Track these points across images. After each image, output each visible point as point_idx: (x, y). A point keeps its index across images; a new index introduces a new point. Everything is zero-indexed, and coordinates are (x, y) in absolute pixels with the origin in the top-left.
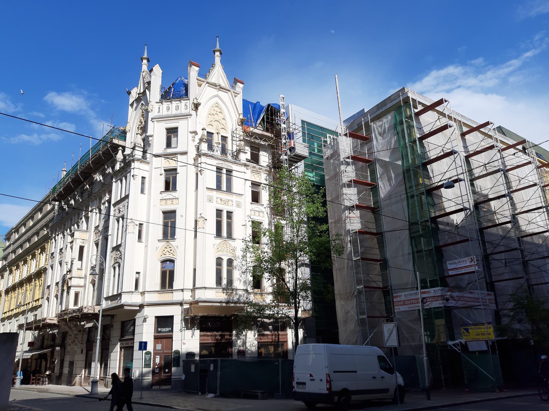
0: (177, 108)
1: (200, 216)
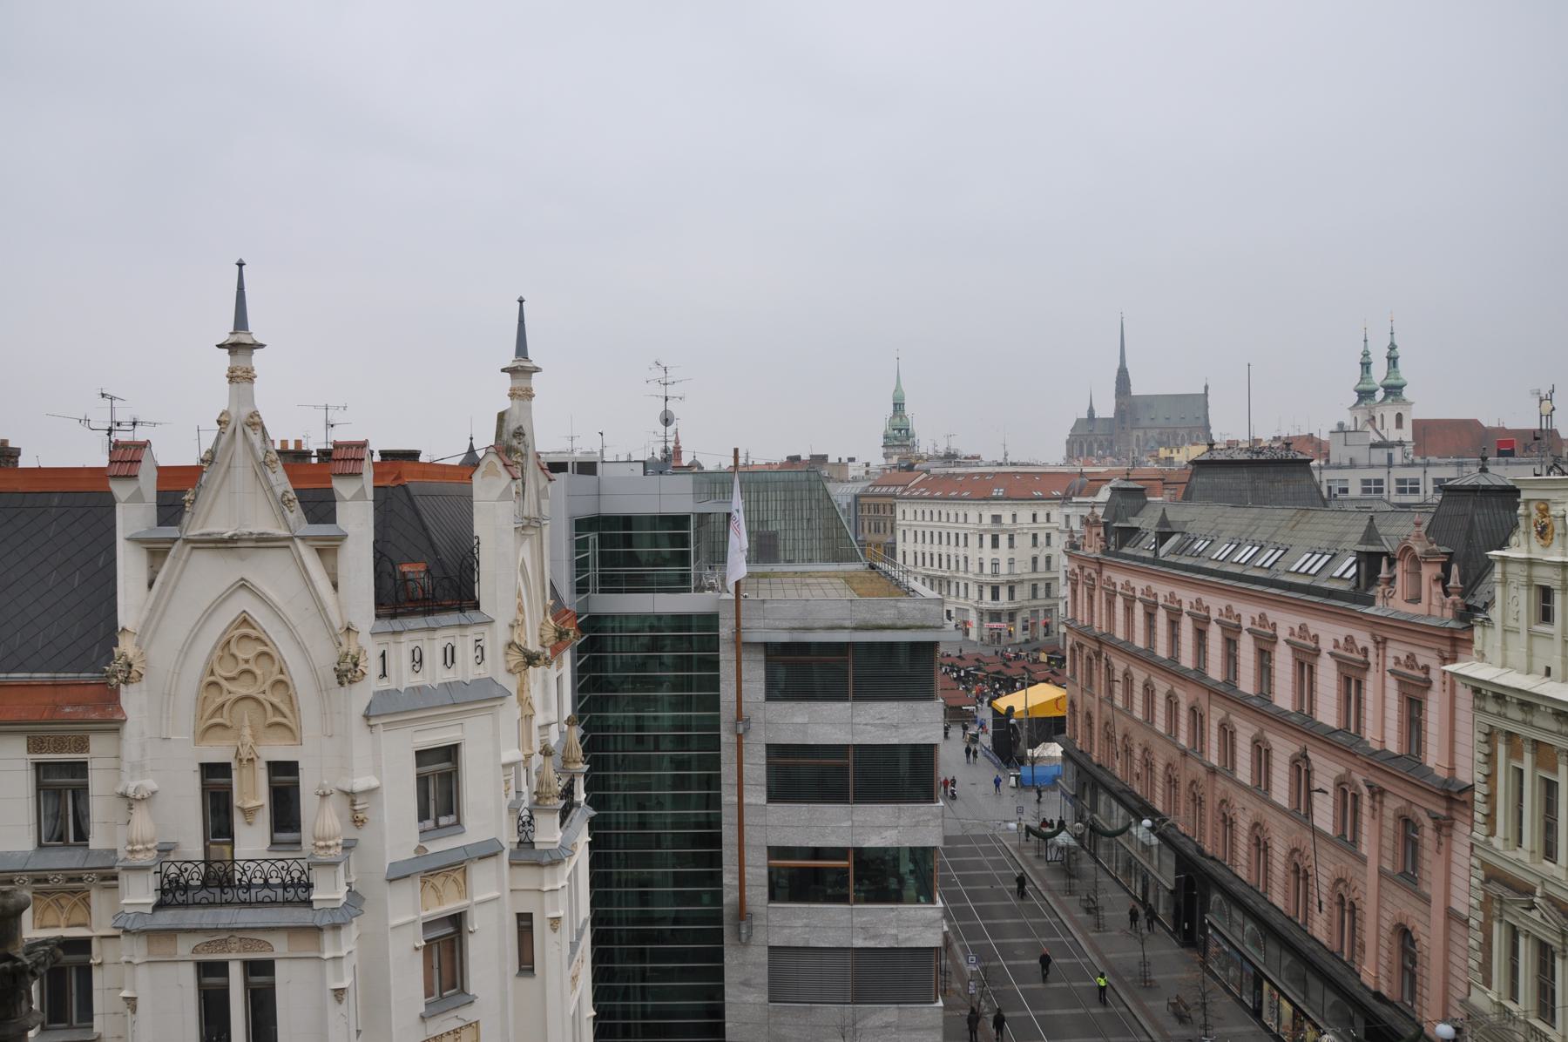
0: (450, 656)
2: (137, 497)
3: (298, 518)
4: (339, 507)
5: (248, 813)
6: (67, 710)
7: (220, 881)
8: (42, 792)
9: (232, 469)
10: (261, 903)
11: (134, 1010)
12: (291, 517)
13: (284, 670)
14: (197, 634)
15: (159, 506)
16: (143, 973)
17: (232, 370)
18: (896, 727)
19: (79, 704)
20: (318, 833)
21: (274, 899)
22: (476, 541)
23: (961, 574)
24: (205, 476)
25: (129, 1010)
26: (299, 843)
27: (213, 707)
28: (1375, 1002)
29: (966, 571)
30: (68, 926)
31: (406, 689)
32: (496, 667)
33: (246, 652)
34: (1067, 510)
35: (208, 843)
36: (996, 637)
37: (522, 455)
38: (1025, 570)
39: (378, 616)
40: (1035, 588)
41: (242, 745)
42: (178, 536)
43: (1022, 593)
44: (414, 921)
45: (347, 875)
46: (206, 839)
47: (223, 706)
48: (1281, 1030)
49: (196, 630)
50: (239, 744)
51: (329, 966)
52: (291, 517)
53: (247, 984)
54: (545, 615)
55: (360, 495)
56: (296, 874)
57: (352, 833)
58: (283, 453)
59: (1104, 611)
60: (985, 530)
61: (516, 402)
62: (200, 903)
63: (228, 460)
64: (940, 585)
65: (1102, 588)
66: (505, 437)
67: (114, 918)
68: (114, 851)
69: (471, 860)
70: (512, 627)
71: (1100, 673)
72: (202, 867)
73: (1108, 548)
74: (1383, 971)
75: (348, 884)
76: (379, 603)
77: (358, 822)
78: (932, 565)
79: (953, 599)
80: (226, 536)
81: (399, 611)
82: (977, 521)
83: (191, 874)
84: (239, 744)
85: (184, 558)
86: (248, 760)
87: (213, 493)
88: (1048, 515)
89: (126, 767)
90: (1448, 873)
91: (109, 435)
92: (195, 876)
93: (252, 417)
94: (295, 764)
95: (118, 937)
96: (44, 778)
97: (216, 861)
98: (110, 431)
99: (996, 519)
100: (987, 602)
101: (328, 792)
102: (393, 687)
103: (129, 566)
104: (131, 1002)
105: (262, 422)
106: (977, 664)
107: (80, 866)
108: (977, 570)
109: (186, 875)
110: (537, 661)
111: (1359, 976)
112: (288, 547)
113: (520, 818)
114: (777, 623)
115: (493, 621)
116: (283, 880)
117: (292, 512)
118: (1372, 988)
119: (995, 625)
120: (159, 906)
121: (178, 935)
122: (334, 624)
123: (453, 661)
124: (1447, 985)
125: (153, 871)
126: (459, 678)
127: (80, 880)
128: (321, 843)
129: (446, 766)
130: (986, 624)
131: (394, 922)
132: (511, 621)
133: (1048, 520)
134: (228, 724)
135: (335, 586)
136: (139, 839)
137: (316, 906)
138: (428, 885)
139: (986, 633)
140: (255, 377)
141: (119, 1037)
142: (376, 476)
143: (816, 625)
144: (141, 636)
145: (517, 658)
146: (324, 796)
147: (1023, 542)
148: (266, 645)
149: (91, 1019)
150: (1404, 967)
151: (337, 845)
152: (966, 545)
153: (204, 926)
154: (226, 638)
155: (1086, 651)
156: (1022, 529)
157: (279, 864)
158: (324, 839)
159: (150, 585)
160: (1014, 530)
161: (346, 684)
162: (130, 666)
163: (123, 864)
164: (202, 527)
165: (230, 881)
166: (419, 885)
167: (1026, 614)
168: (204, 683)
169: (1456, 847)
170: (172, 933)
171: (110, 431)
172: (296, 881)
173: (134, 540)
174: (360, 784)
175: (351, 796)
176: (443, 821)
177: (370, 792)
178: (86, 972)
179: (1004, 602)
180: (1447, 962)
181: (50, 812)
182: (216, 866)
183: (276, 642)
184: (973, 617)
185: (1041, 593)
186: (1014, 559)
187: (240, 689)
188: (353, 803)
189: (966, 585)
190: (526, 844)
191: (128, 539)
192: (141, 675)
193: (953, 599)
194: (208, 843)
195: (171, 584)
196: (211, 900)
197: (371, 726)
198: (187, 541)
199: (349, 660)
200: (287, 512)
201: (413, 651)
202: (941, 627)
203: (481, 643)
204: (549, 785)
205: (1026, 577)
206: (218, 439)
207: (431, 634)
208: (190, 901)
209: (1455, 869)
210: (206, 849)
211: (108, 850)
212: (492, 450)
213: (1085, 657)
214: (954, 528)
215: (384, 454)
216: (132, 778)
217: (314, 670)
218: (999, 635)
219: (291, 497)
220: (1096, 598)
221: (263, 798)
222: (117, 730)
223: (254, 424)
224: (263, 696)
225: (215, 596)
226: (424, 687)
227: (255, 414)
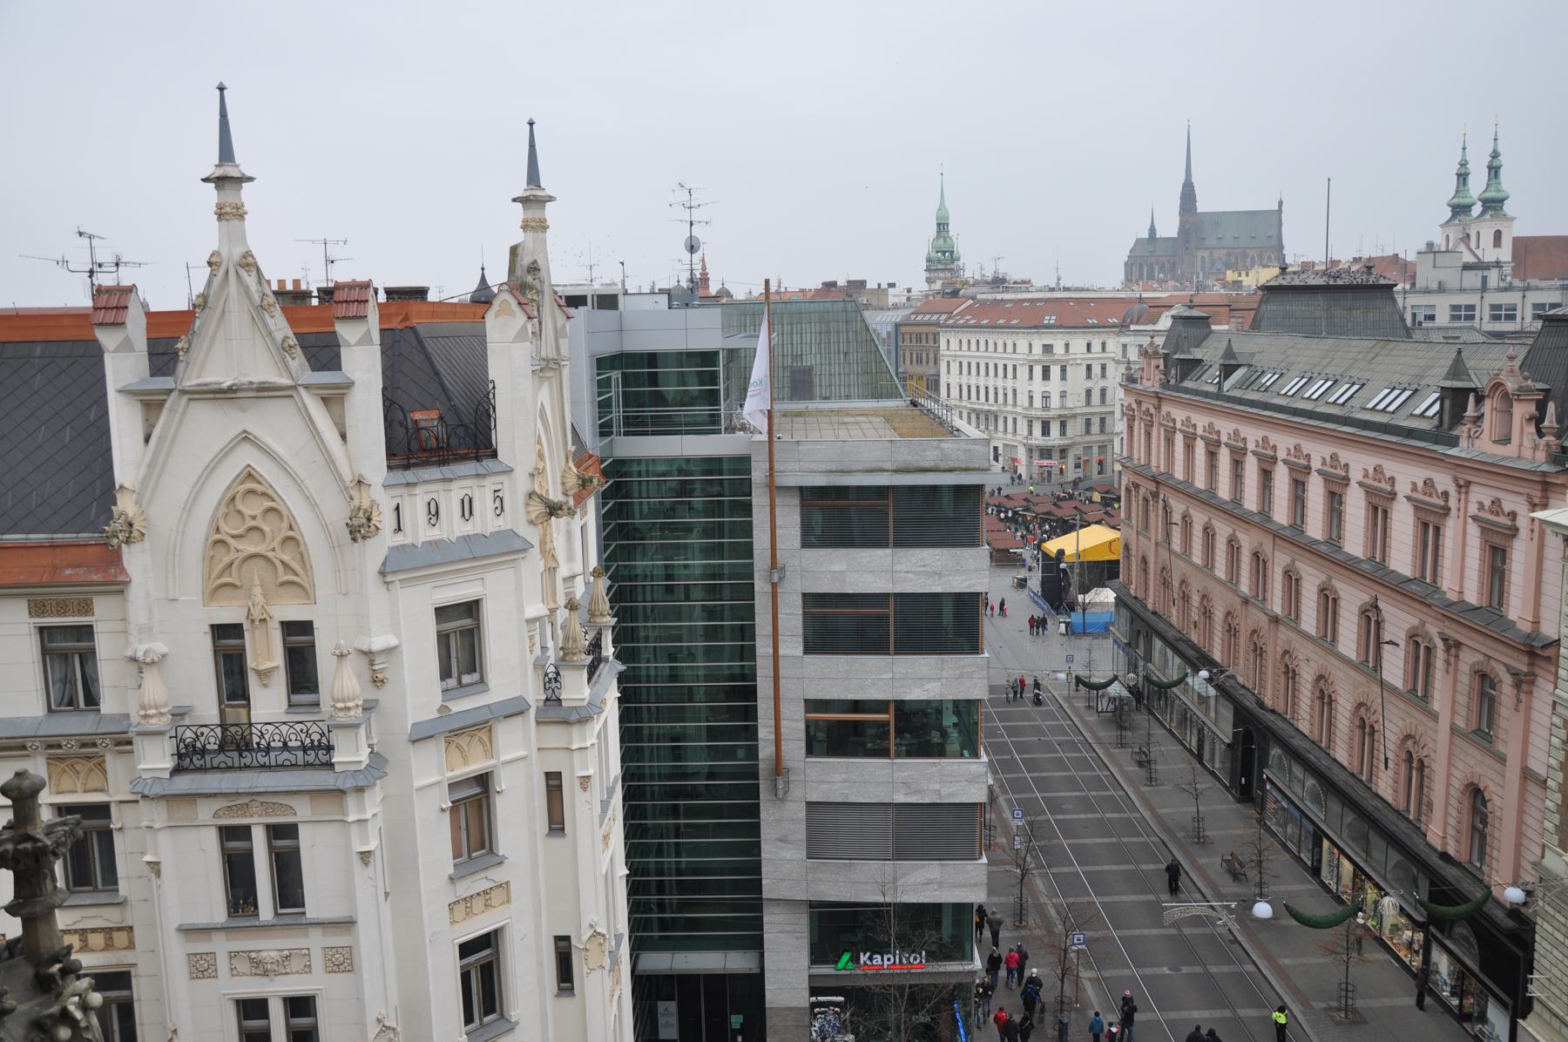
0: (467, 509)
1: (590, 932)
2: (126, 346)
4: (344, 352)
5: (264, 675)
6: (68, 572)
7: (238, 745)
8: (48, 657)
9: (226, 314)
10: (280, 767)
11: (158, 874)
12: (293, 364)
13: (296, 529)
14: (199, 491)
15: (150, 354)
16: (164, 839)
17: (220, 207)
18: (939, 575)
19: (80, 566)
20: (337, 694)
22: (491, 386)
23: (1009, 408)
24: (198, 322)
26: (317, 705)
27: (221, 566)
28: (1441, 863)
29: (1015, 404)
30: (85, 792)
31: (423, 543)
32: (517, 519)
33: (253, 508)
34: (1124, 340)
36: (1047, 476)
37: (538, 292)
38: (1078, 404)
39: (390, 468)
40: (1088, 423)
41: (253, 605)
42: (173, 386)
43: (1076, 428)
44: (439, 783)
46: (220, 703)
48: (1341, 889)
49: (198, 487)
50: (250, 604)
51: (354, 829)
52: (293, 364)
53: (270, 847)
54: (567, 461)
55: (365, 340)
56: (316, 737)
57: (372, 694)
58: (280, 294)
59: (1162, 449)
60: (1036, 361)
61: (530, 234)
62: (218, 768)
63: (222, 303)
64: (987, 419)
65: (1160, 424)
66: (519, 273)
67: (131, 783)
69: (496, 719)
70: (532, 475)
71: (1157, 516)
72: (218, 730)
73: (1168, 381)
74: (1451, 831)
75: (370, 746)
76: (391, 454)
77: (377, 682)
78: (978, 399)
79: (1000, 435)
80: (225, 386)
81: (412, 461)
82: (1027, 351)
84: (250, 604)
85: (181, 409)
86: (260, 620)
87: (208, 339)
88: (1104, 344)
89: (133, 629)
90: (1527, 732)
91: (90, 277)
92: (212, 740)
93: (244, 257)
94: (311, 623)
95: (137, 802)
96: (49, 642)
97: (233, 725)
98: (91, 272)
99: (1048, 349)
100: (1038, 438)
101: (345, 652)
102: (408, 541)
103: (123, 420)
104: (155, 867)
105: (256, 263)
106: (1025, 504)
107: (93, 732)
108: (1026, 404)
109: (202, 739)
110: (559, 512)
111: (1425, 836)
112: (292, 396)
113: (546, 675)
114: (813, 466)
115: (512, 470)
117: (294, 359)
118: (1439, 848)
119: (1045, 462)
120: (177, 771)
121: (198, 800)
122: (345, 478)
123: (471, 513)
124: (1519, 846)
125: (167, 736)
126: (478, 531)
127: (94, 745)
128: (340, 705)
129: (466, 622)
130: (1036, 461)
131: (418, 783)
132: (531, 470)
133: (1104, 350)
134: (237, 583)
135: (343, 437)
136: (152, 702)
137: (338, 768)
138: (453, 746)
139: (1036, 471)
140: (246, 213)
142: (382, 318)
143: (854, 468)
144: (140, 495)
145: (538, 508)
146: (341, 656)
147: (1076, 374)
148: (274, 501)
149: (115, 882)
150: (1474, 828)
151: (357, 706)
152: (1015, 377)
153: (224, 791)
154: (230, 494)
155: (1142, 491)
156: (1075, 359)
157: (298, 727)
158: (343, 701)
159: (147, 440)
160: (1067, 361)
162: (131, 525)
164: (199, 376)
165: (248, 747)
166: (443, 745)
167: (1079, 451)
168: (209, 542)
169: (1536, 704)
170: (191, 797)
171: (91, 272)
172: (316, 743)
173: (125, 392)
174: (378, 642)
175: (369, 655)
176: (466, 679)
177: (390, 651)
178: (107, 837)
179: (1055, 438)
180: (1520, 822)
181: (57, 676)
182: (233, 729)
183: (283, 496)
184: (1021, 454)
185: (1095, 428)
186: (1066, 392)
188: (372, 663)
189: (1015, 419)
190: (553, 701)
191: (120, 391)
192: (143, 535)
193: (1000, 435)
194: (223, 707)
196: (230, 764)
197: (387, 583)
198: (183, 392)
200: (289, 358)
201: (429, 504)
202: (988, 469)
203: (500, 494)
204: (575, 640)
205: (1079, 411)
207: (447, 485)
208: (208, 766)
209: (1534, 727)
210: (222, 712)
211: (121, 715)
212: (505, 287)
213: (1141, 497)
214: (1002, 358)
215: (389, 292)
216: (140, 641)
217: (325, 527)
218: (1050, 473)
219: (292, 343)
220: (1154, 434)
221: (278, 659)
222: (122, 592)
223: (248, 265)
224: (273, 553)
225: (216, 449)
226: (442, 540)
227: (248, 254)
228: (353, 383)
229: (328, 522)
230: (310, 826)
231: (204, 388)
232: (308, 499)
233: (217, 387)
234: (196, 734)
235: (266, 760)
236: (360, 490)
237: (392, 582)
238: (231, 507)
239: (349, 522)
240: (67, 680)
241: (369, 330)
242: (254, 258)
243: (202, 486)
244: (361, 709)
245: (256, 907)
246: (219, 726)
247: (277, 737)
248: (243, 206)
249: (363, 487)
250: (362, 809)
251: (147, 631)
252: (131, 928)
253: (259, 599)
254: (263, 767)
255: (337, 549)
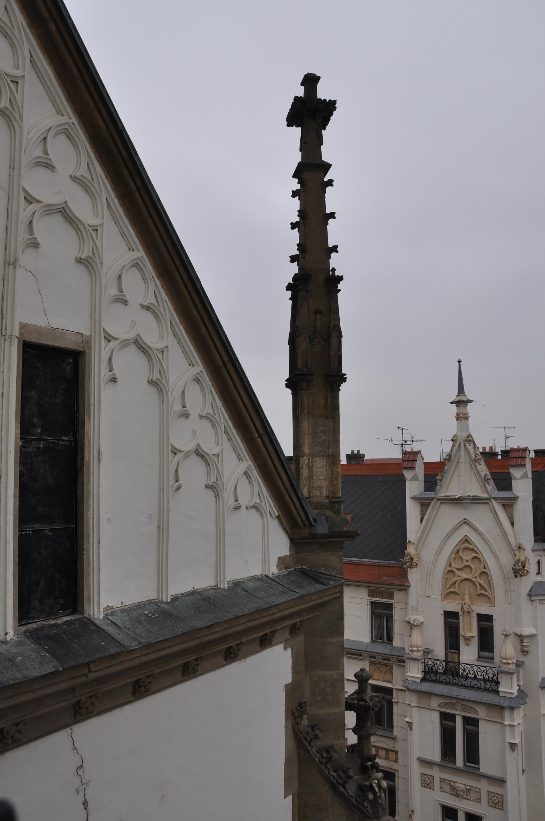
2: (415, 478)
3: (493, 488)
4: (514, 482)
5: (468, 639)
6: (385, 578)
7: (452, 673)
8: (373, 615)
9: (459, 464)
11: (411, 729)
13: (487, 568)
14: (443, 545)
16: (415, 711)
17: (458, 414)
20: (503, 655)
21: (479, 687)
24: (446, 467)
25: (409, 728)
26: (492, 659)
30: (383, 681)
33: (467, 556)
35: (447, 652)
39: (535, 541)
41: (465, 604)
42: (433, 496)
45: (518, 680)
46: (446, 650)
47: (455, 583)
49: (442, 544)
50: (463, 603)
51: (508, 729)
52: (489, 488)
53: (464, 729)
55: (525, 476)
56: (491, 676)
57: (521, 658)
58: (484, 454)
63: (457, 459)
67: (403, 681)
68: (404, 649)
72: (444, 663)
75: (519, 686)
76: (536, 534)
77: (524, 652)
80: (457, 497)
83: (439, 666)
84: (463, 603)
85: (437, 507)
86: (468, 612)
87: (450, 475)
89: (410, 608)
91: (402, 447)
92: (441, 668)
93: (468, 437)
94: (492, 616)
95: (404, 691)
96: (374, 609)
97: (451, 662)
98: (402, 445)
101: (508, 634)
104: (410, 724)
107: (389, 653)
109: (436, 666)
112: (488, 503)
116: (484, 677)
117: (489, 485)
120: (423, 680)
121: (432, 696)
122: (512, 543)
125: (420, 662)
127: (389, 660)
128: (504, 661)
134: (458, 592)
135: (512, 524)
136: (415, 645)
137: (501, 694)
140: (469, 417)
141: (404, 740)
142: (533, 465)
144: (417, 545)
148: (477, 553)
149: (392, 728)
151: (513, 663)
153: (444, 694)
157: (483, 669)
158: (506, 659)
159: (422, 520)
161: (519, 577)
162: (412, 559)
163: (407, 656)
164: (445, 493)
168: (446, 572)
170: (429, 694)
171: (402, 445)
172: (491, 679)
174: (526, 631)
175: (521, 637)
177: (532, 636)
178: (390, 705)
181: (376, 626)
182: (451, 664)
183: (482, 552)
187: (464, 575)
188: (522, 642)
191: (411, 498)
192: (417, 564)
194: (447, 652)
195: (431, 521)
196: (448, 681)
197: (532, 601)
198: (438, 499)
199: (520, 564)
200: (487, 485)
206: (452, 449)
210: (446, 655)
211: (401, 648)
215: (536, 452)
217: (501, 568)
219: (489, 477)
221: (474, 633)
222: (406, 590)
223: (470, 441)
227: (470, 436)
228: (518, 498)
229: (503, 567)
230: (485, 722)
231: (448, 498)
232: (494, 554)
233: (454, 497)
234: (434, 663)
235: (465, 682)
236: (520, 552)
237: (534, 600)
238: (457, 555)
239: (514, 567)
240: (380, 628)
241: (526, 471)
242: (472, 438)
243: (445, 543)
244: (515, 664)
245: (455, 758)
246: (444, 661)
247: (471, 672)
248: (468, 414)
249: (521, 550)
250: (513, 719)
251: (415, 610)
252: (397, 752)
253: (468, 601)
254: (464, 686)
255: (507, 580)
